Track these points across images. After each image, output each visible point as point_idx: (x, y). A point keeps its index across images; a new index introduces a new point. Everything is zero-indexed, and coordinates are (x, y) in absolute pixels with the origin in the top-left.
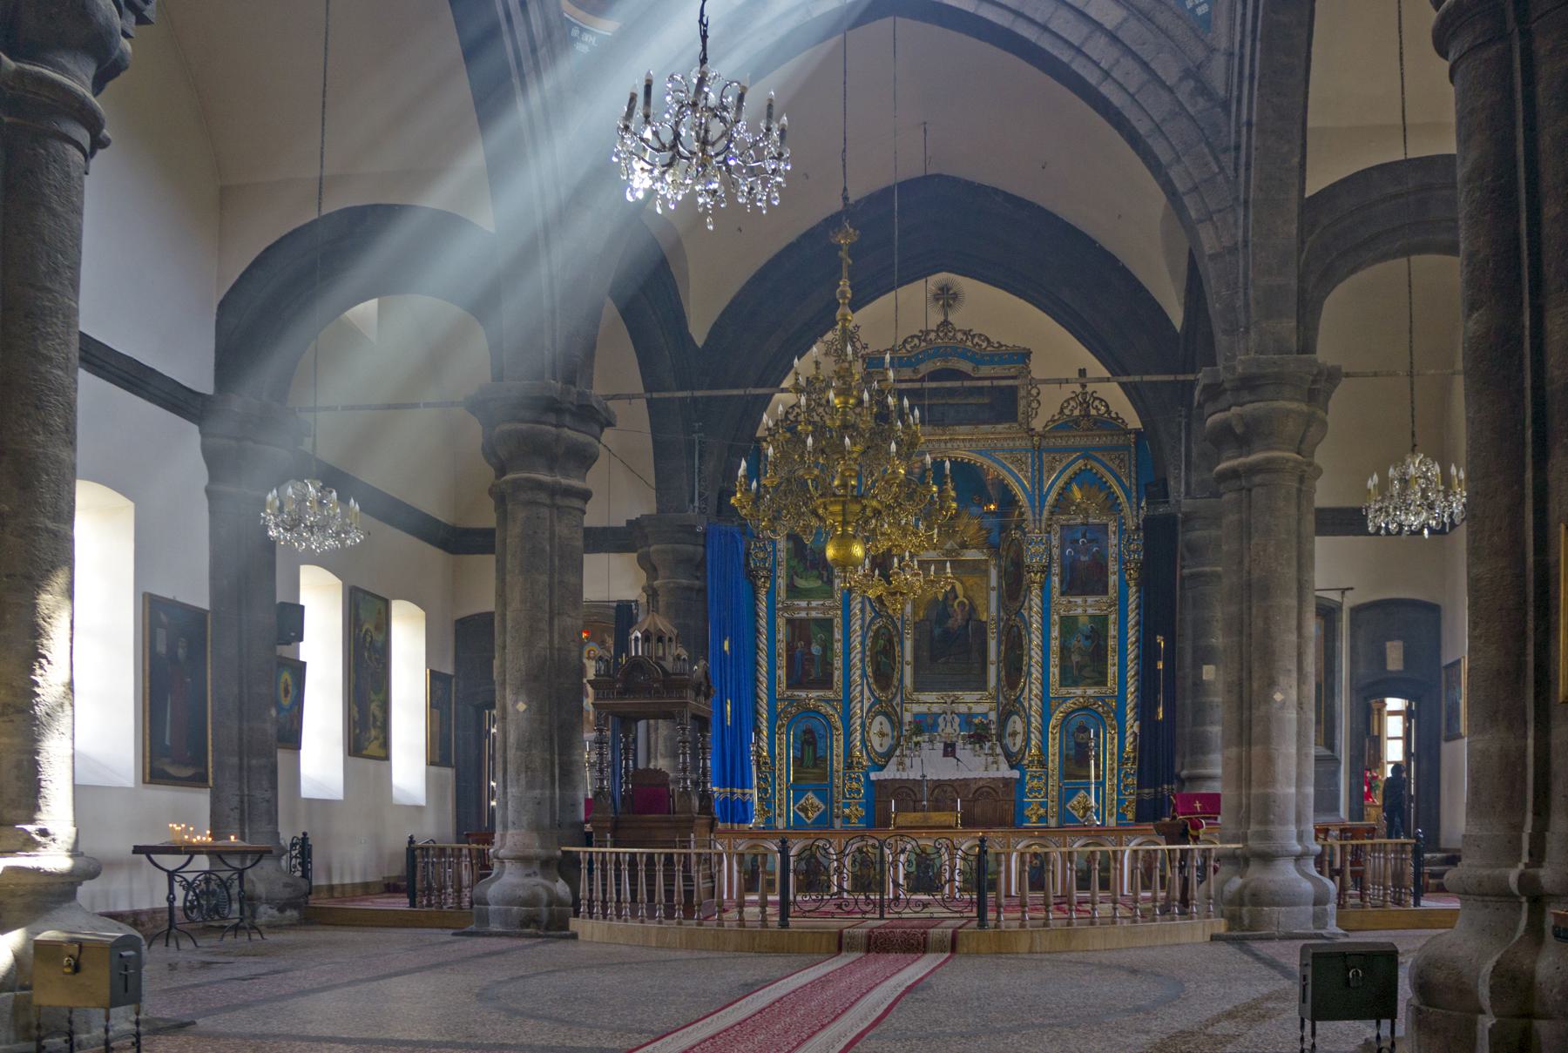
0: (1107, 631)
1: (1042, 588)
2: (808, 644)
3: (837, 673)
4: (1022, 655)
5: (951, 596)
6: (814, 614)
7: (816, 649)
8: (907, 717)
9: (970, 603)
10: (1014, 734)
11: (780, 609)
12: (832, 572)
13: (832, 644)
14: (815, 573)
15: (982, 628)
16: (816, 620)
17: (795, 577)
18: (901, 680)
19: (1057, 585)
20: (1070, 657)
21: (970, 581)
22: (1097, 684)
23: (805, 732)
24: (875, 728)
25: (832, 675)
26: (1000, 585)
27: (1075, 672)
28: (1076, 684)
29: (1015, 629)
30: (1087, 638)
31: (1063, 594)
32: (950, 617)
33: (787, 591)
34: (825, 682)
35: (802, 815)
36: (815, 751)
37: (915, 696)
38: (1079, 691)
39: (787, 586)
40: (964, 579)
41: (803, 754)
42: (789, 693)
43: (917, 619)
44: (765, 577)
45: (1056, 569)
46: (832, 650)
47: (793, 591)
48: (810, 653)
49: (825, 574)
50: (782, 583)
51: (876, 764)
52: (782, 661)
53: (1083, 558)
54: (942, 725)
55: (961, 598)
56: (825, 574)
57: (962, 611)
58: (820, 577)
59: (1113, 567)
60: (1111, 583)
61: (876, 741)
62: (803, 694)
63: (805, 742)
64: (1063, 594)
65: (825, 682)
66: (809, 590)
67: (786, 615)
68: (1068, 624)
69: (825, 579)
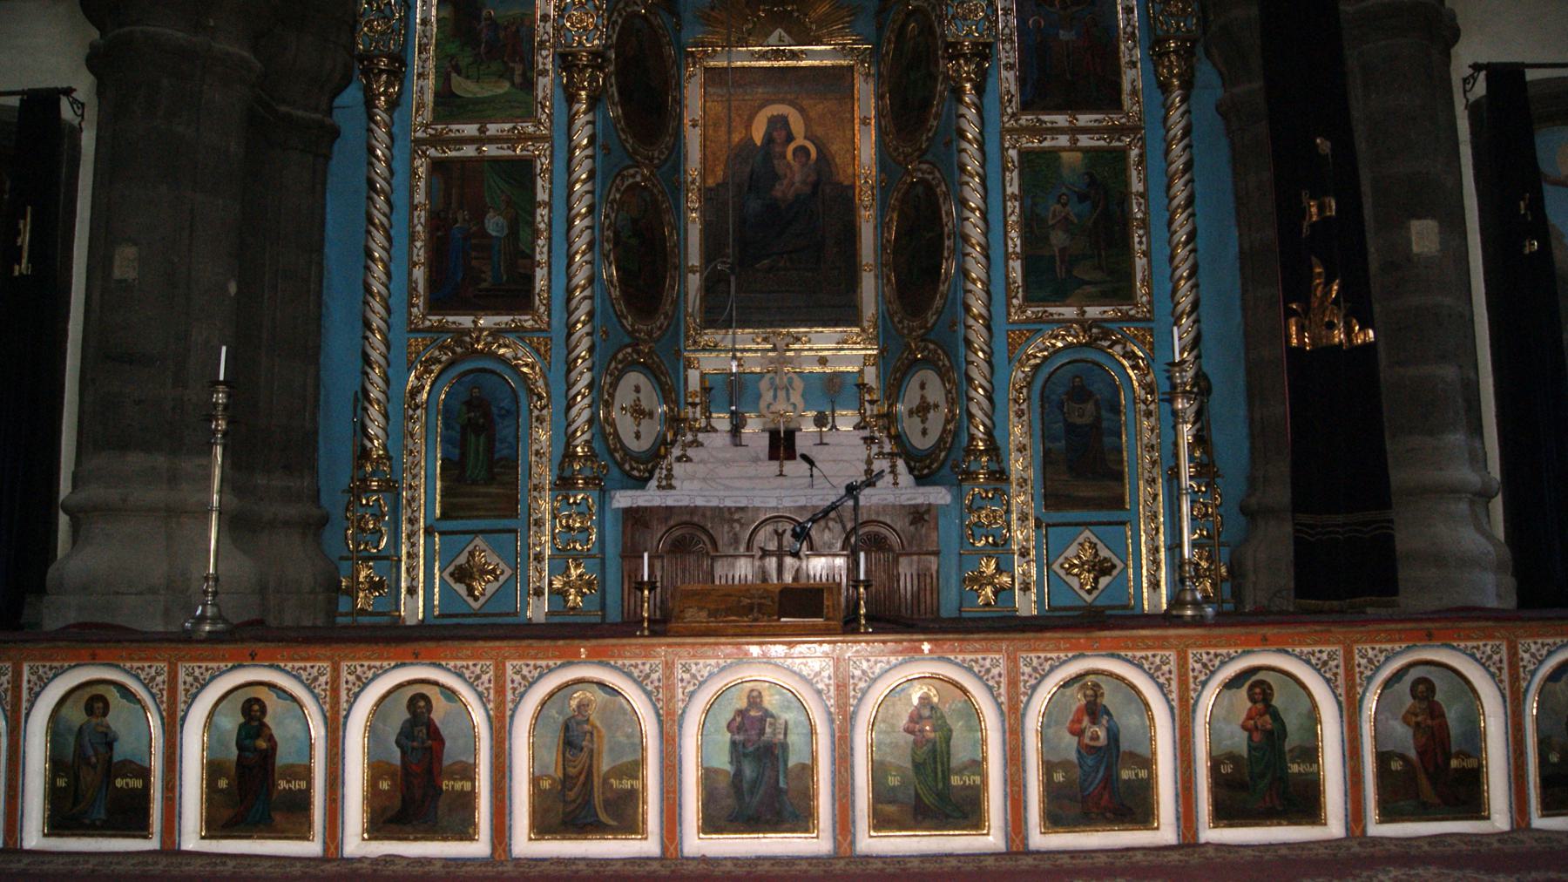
0: (1127, 183)
1: (980, 89)
2: (479, 216)
3: (540, 274)
4: (941, 237)
5: (779, 136)
6: (489, 150)
7: (494, 224)
8: (694, 377)
9: (819, 150)
10: (923, 409)
11: (418, 142)
12: (531, 65)
13: (533, 215)
14: (495, 66)
15: (845, 200)
16: (495, 161)
17: (454, 75)
18: (675, 302)
19: (1013, 89)
20: (1047, 238)
21: (818, 109)
22: (1103, 298)
23: (469, 404)
24: (624, 395)
25: (530, 279)
26: (880, 115)
27: (1060, 272)
28: (1061, 297)
29: (920, 189)
30: (1082, 198)
31: (1026, 107)
32: (776, 177)
33: (436, 104)
34: (516, 295)
35: (461, 589)
36: (490, 449)
37: (709, 336)
38: (1070, 312)
39: (437, 95)
40: (806, 103)
41: (463, 455)
42: (434, 319)
43: (711, 182)
44: (388, 72)
45: (1007, 53)
46: (532, 223)
47: (449, 105)
48: (483, 233)
49: (518, 69)
50: (423, 86)
51: (630, 476)
52: (420, 252)
53: (1064, 35)
54: (768, 396)
55: (800, 141)
56: (518, 69)
57: (803, 165)
58: (506, 74)
59: (1131, 53)
60: (1126, 86)
61: (625, 425)
62: (466, 321)
63: (470, 427)
64: (1026, 107)
65: (516, 295)
66: (483, 101)
67: (432, 152)
68: (1037, 167)
69: (517, 80)
